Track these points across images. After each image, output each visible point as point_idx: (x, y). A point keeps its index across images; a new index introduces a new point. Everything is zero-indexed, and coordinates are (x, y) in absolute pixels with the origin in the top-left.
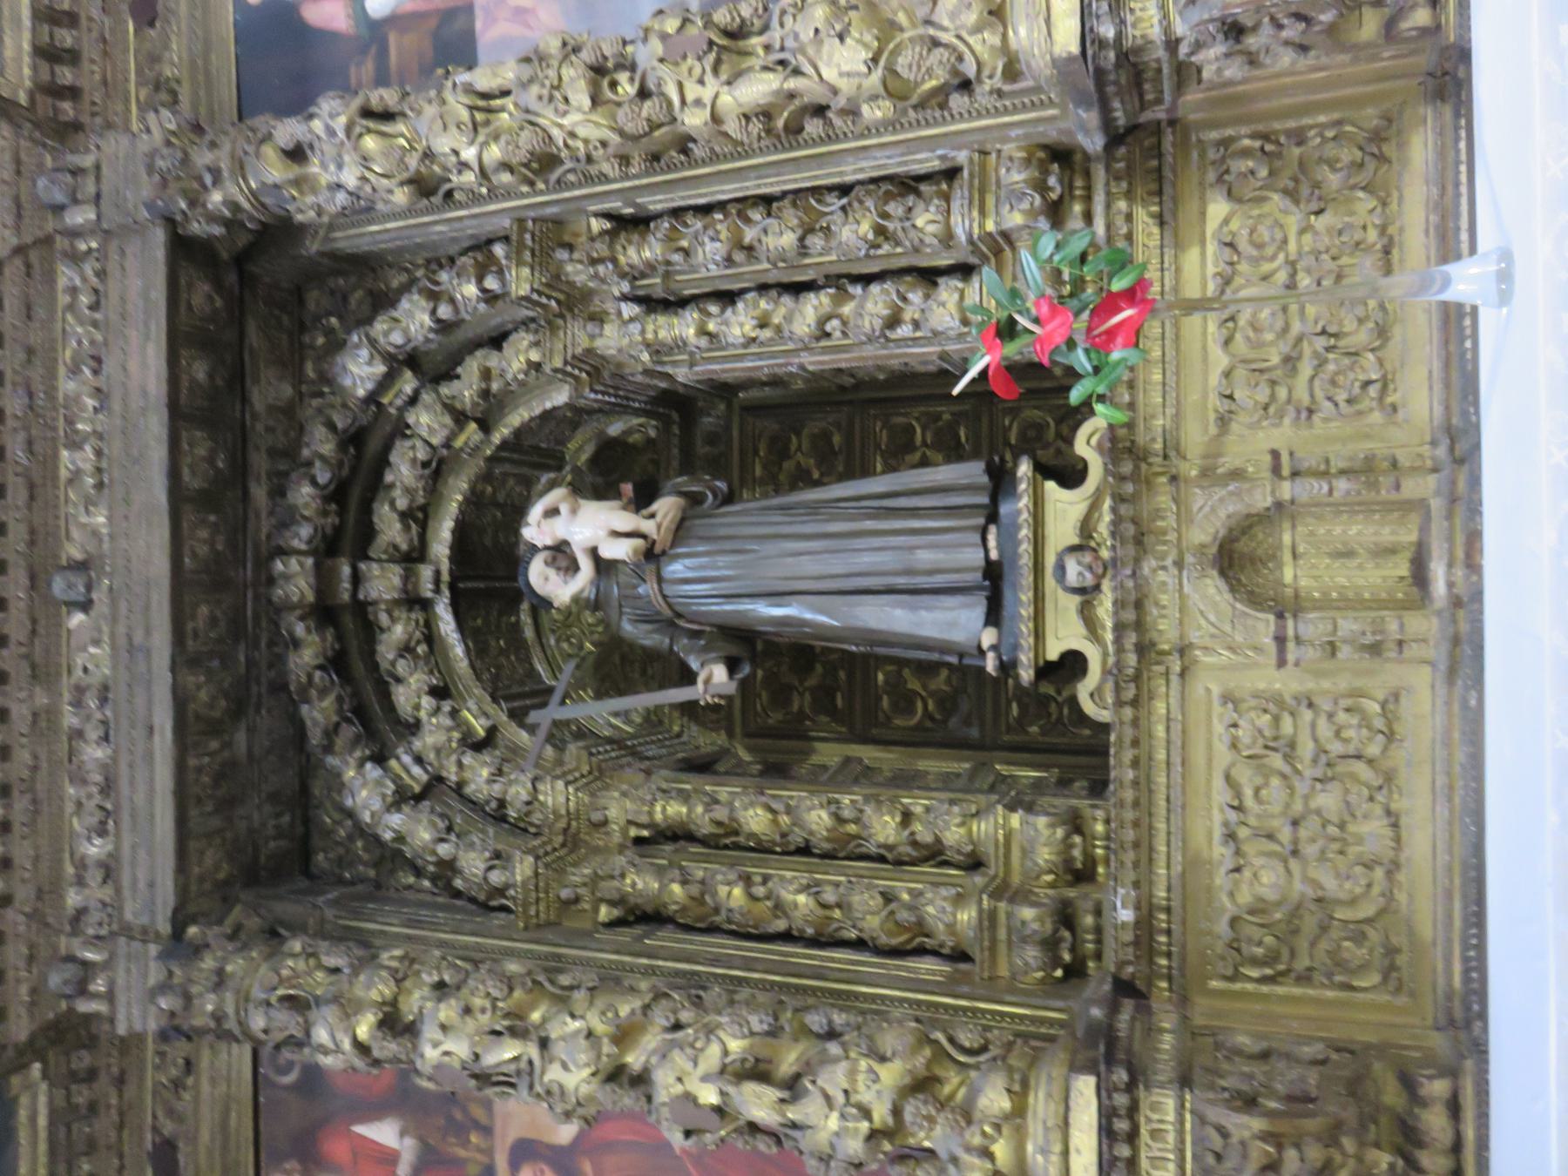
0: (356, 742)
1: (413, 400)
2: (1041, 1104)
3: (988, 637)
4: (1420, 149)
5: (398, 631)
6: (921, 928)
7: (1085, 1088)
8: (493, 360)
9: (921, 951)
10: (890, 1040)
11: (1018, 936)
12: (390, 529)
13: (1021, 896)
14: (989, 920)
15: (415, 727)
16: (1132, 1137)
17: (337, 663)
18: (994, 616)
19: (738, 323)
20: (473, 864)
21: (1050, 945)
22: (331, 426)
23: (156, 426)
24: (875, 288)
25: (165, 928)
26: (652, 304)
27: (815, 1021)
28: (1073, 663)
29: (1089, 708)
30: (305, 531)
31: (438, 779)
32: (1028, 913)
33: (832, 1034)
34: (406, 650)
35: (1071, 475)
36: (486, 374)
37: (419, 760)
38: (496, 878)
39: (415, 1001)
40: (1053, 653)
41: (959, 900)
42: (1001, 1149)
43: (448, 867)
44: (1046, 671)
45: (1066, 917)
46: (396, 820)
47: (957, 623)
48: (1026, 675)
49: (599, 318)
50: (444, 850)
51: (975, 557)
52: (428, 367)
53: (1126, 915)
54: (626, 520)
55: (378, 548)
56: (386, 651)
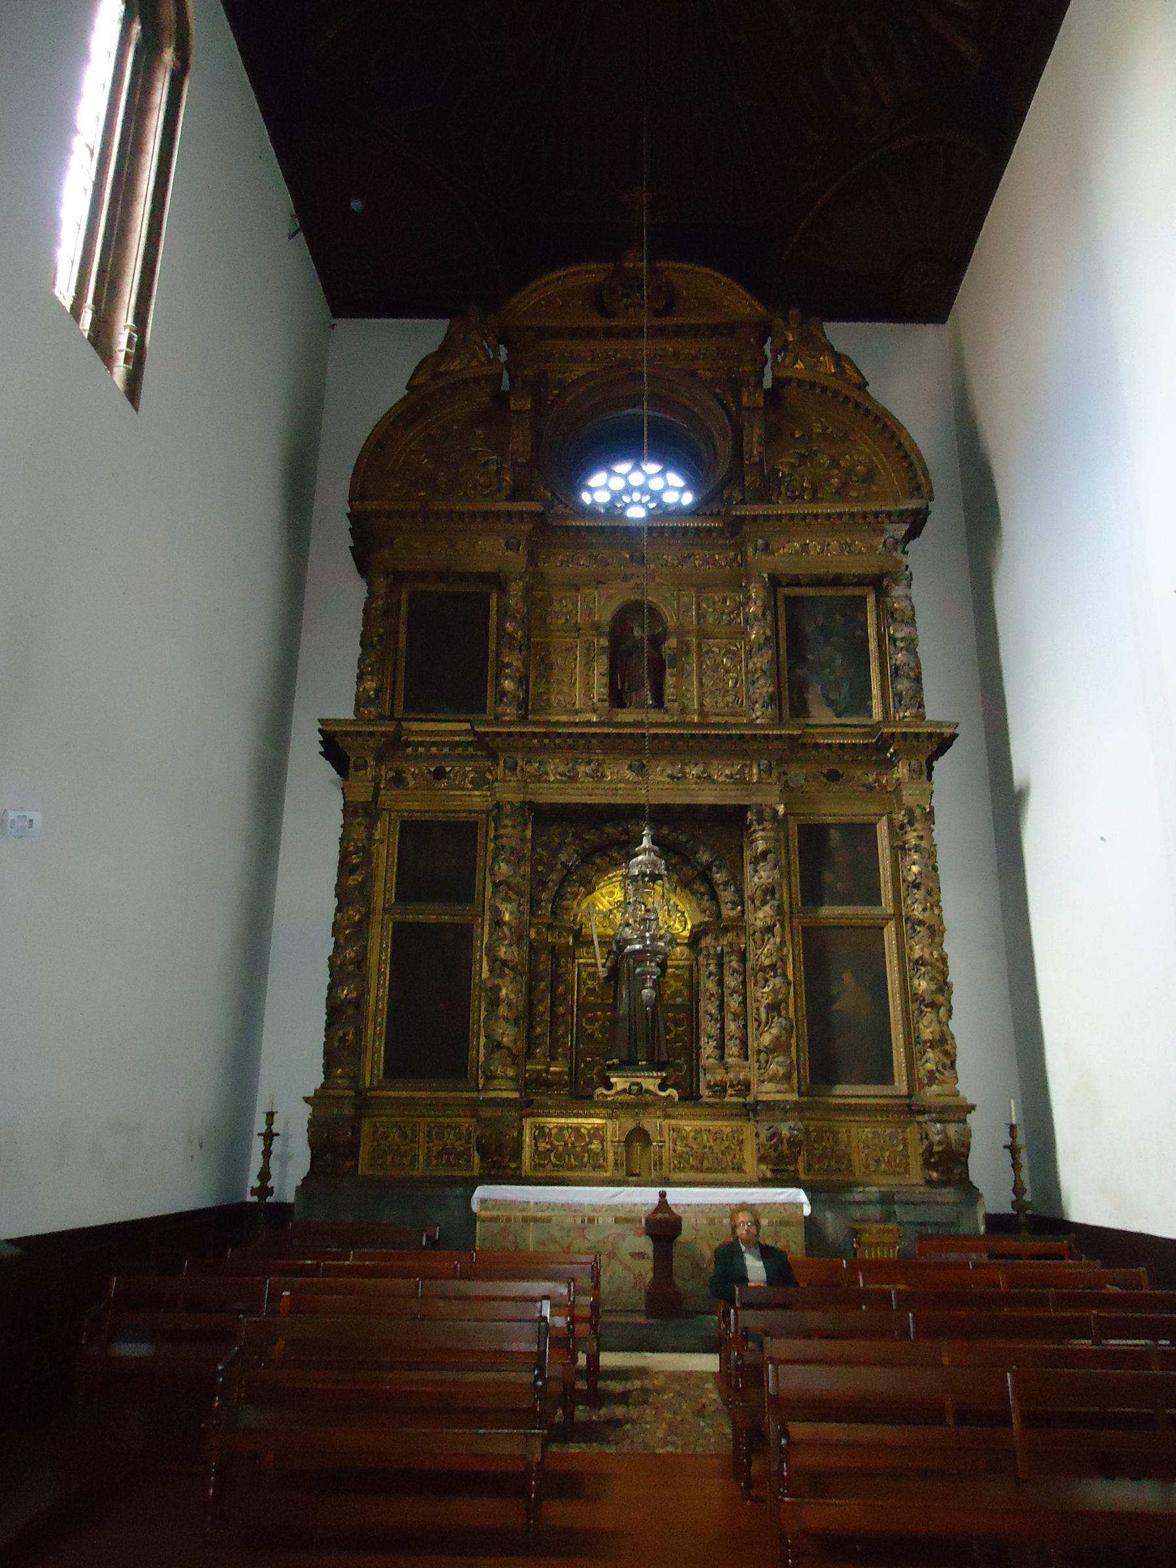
7: (516, 1095)
19: (711, 986)
28: (610, 1086)
35: (662, 1087)
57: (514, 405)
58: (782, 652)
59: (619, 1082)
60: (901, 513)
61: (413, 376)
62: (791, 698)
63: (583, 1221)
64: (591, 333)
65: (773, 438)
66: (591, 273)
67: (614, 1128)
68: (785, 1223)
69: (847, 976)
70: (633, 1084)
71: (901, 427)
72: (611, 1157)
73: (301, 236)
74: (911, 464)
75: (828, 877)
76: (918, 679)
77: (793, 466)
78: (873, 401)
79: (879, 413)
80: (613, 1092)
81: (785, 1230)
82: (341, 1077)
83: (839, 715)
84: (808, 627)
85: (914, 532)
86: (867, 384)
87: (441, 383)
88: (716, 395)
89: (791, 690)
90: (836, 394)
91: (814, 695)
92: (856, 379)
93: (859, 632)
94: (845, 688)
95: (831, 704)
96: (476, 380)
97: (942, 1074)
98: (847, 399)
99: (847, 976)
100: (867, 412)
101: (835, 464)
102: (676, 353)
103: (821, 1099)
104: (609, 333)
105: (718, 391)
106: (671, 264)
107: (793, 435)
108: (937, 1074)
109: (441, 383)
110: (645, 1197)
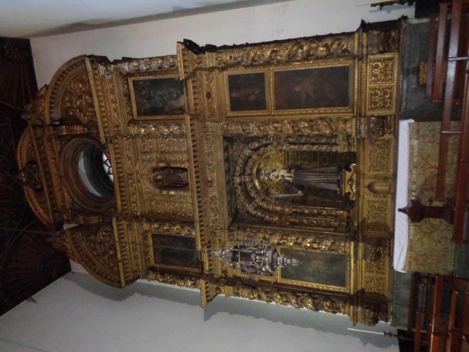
0: (247, 202)
1: (253, 154)
2: (347, 244)
3: (338, 189)
4: (393, 143)
5: (251, 185)
6: (331, 225)
7: (352, 243)
8: (266, 149)
9: (330, 227)
10: (330, 239)
11: (343, 226)
12: (248, 171)
13: (343, 221)
14: (339, 224)
15: (254, 199)
16: (357, 247)
17: (242, 191)
18: (339, 186)
20: (267, 217)
21: (346, 227)
22: (242, 159)
23: (222, 163)
24: (324, 146)
25: (227, 228)
26: (291, 143)
27: (320, 237)
28: (349, 193)
29: (351, 199)
30: (238, 173)
31: (258, 206)
32: (344, 223)
33: (323, 238)
34: (252, 188)
35: (349, 170)
36: (264, 150)
37: (256, 203)
38: (271, 219)
39: (267, 236)
40: (346, 192)
41: (335, 222)
42: (343, 249)
43: (263, 218)
44: (346, 194)
45: (348, 223)
46: (255, 212)
47: (334, 187)
48: (343, 195)
49: (282, 145)
50: (263, 216)
51: (336, 179)
52: (256, 150)
53: (356, 224)
54: (289, 175)
55: (246, 173)
56: (249, 188)
57: (82, 222)
58: (160, 117)
59: (348, 190)
60: (94, 69)
61: (76, 262)
62: (178, 114)
63: (412, 226)
64: (51, 192)
65: (78, 122)
66: (29, 192)
67: (368, 196)
68: (418, 131)
69: (297, 89)
70: (348, 183)
71: (59, 70)
72: (382, 199)
73: (34, 297)
74: (74, 64)
75: (253, 98)
76: (162, 58)
77: (84, 115)
78: (52, 81)
79: (56, 80)
80: (351, 192)
81: (422, 132)
82: (345, 310)
83: (183, 93)
84: (148, 106)
85: (103, 60)
86: (46, 85)
87: (76, 253)
88: (66, 144)
89: (175, 114)
90: (52, 98)
91: (175, 104)
92: (44, 89)
93: (148, 84)
94: (172, 90)
95: (178, 96)
96: (73, 239)
97: (343, 46)
98: (53, 93)
99: (297, 89)
100: (56, 84)
101: (80, 97)
102: (53, 158)
103: (355, 103)
104: (50, 186)
105: (64, 143)
106: (20, 164)
107: (73, 115)
108: (343, 48)
109: (76, 253)
110: (402, 226)
